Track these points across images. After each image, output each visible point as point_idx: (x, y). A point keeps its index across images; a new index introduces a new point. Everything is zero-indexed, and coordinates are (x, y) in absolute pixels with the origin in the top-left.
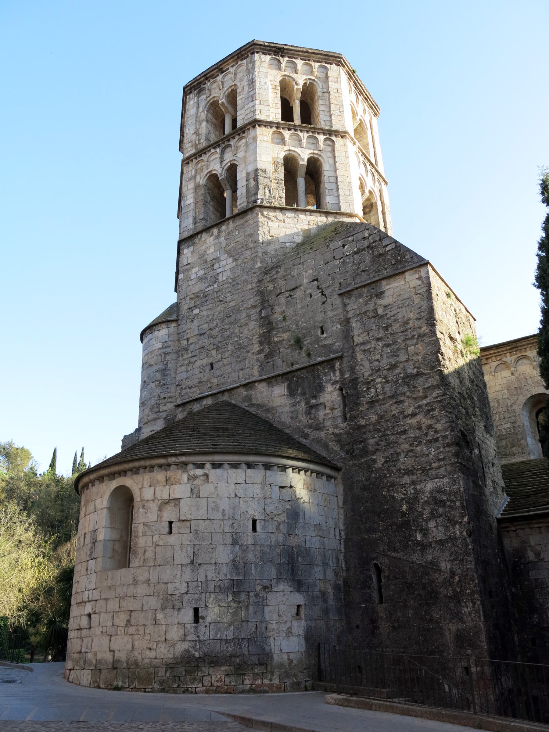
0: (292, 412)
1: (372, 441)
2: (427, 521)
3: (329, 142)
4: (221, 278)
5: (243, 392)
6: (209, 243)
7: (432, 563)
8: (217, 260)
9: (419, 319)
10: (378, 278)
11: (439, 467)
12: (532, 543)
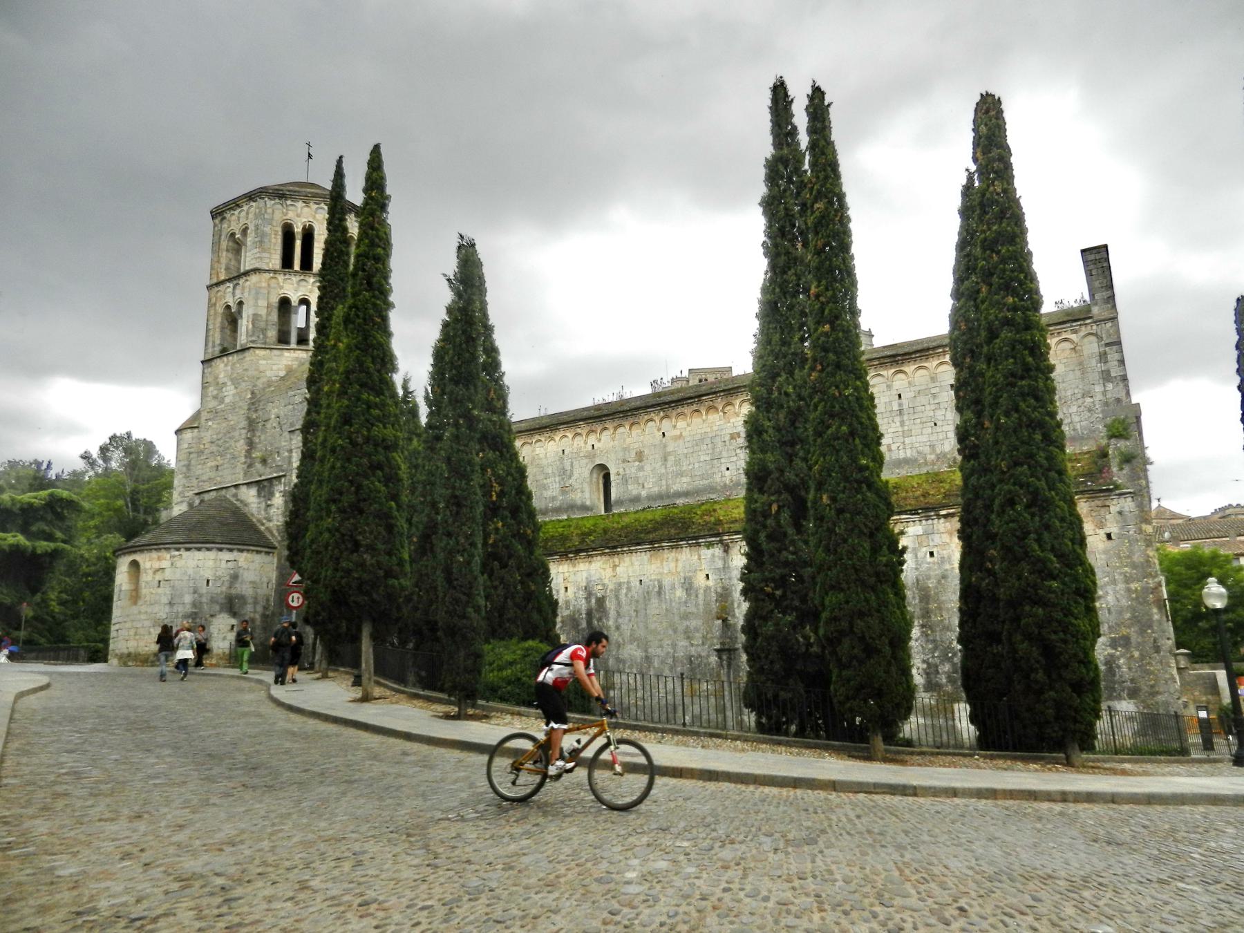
4: (227, 400)
5: (233, 490)
6: (222, 368)
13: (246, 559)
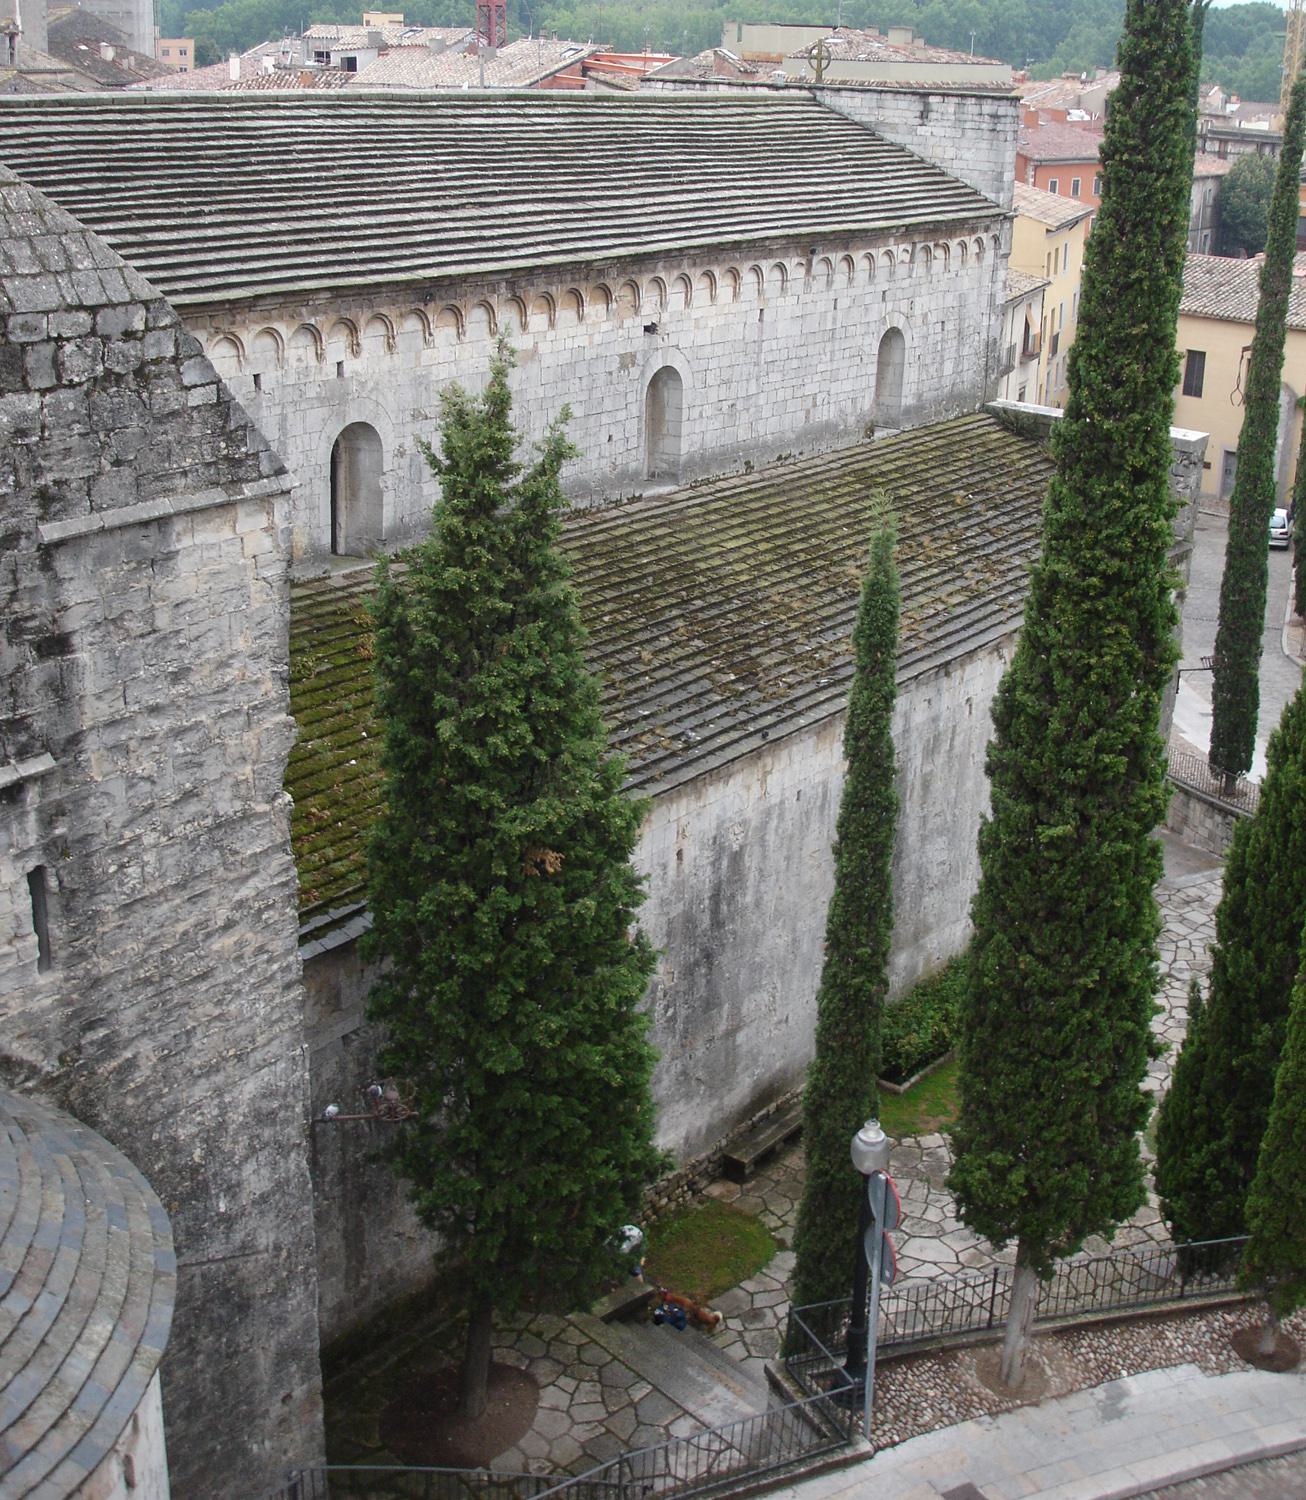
1: (129, 1015)
2: (238, 1167)
7: (243, 1247)
9: (255, 656)
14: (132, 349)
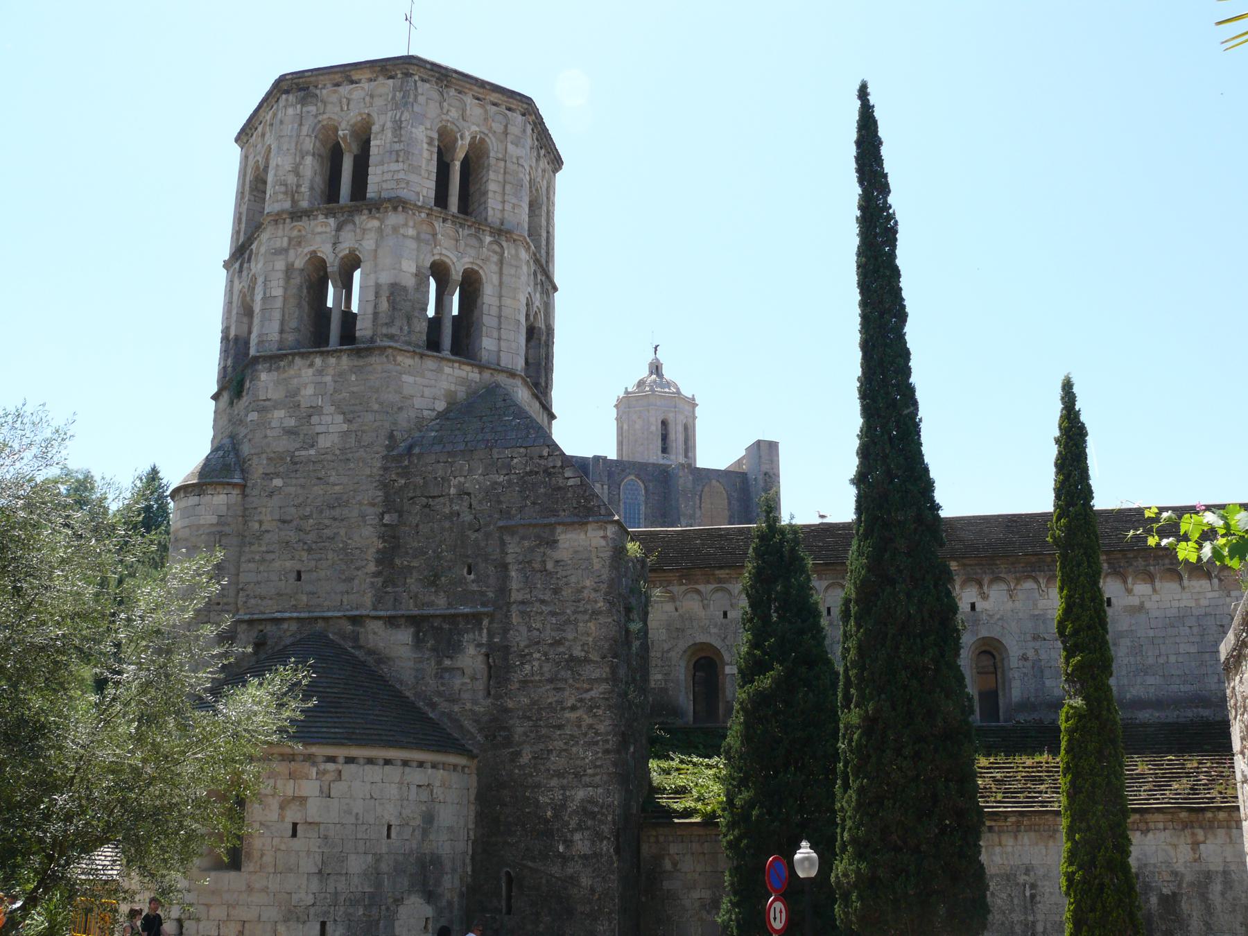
0: (417, 670)
1: (520, 730)
2: (573, 832)
3: (496, 247)
4: (324, 442)
7: (572, 877)
8: (316, 410)
9: (596, 591)
10: (553, 520)
11: (594, 775)
12: (671, 852)
13: (443, 785)
14: (542, 462)
